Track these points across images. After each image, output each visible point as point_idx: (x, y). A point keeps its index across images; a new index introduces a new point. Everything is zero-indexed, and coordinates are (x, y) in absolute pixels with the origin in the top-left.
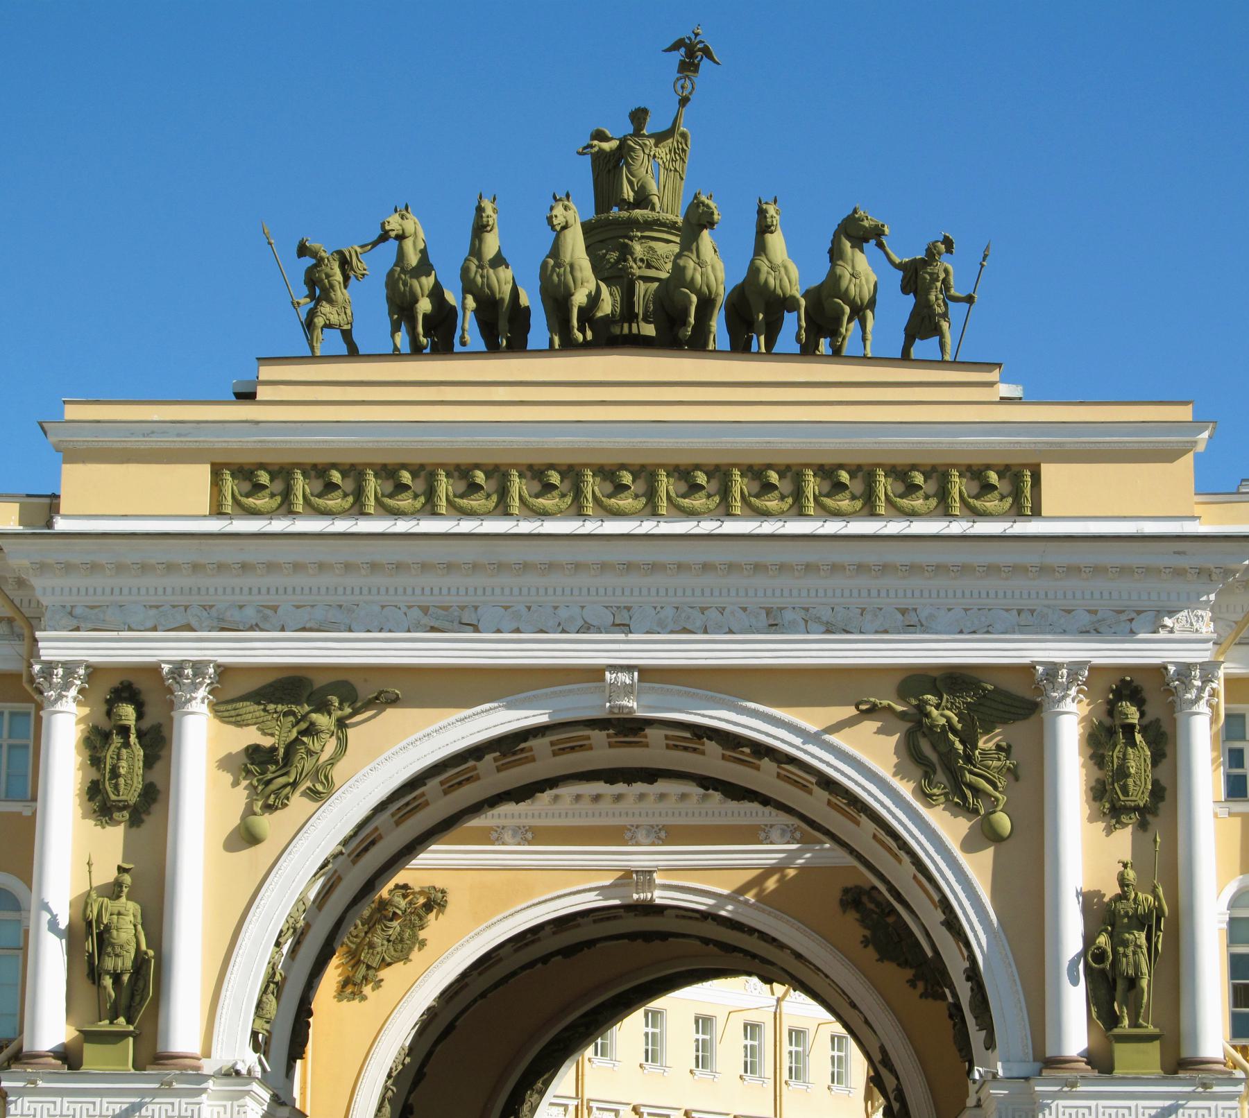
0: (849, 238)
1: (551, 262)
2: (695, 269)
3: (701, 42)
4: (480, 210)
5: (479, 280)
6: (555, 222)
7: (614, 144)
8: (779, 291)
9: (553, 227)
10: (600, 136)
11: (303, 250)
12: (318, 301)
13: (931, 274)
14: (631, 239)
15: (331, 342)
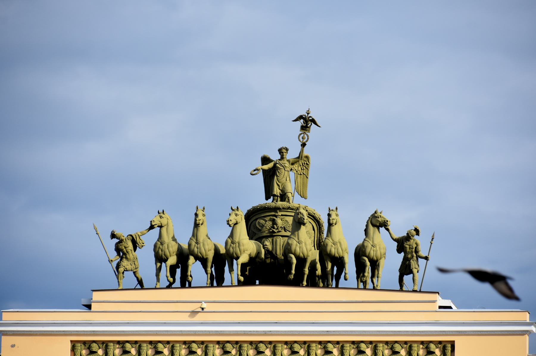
0: (374, 225)
1: (230, 241)
2: (296, 245)
3: (311, 117)
4: (196, 215)
5: (196, 250)
6: (230, 223)
7: (271, 165)
8: (337, 255)
9: (230, 226)
10: (265, 160)
11: (113, 236)
12: (122, 258)
13: (409, 245)
14: (276, 216)
15: (129, 279)
